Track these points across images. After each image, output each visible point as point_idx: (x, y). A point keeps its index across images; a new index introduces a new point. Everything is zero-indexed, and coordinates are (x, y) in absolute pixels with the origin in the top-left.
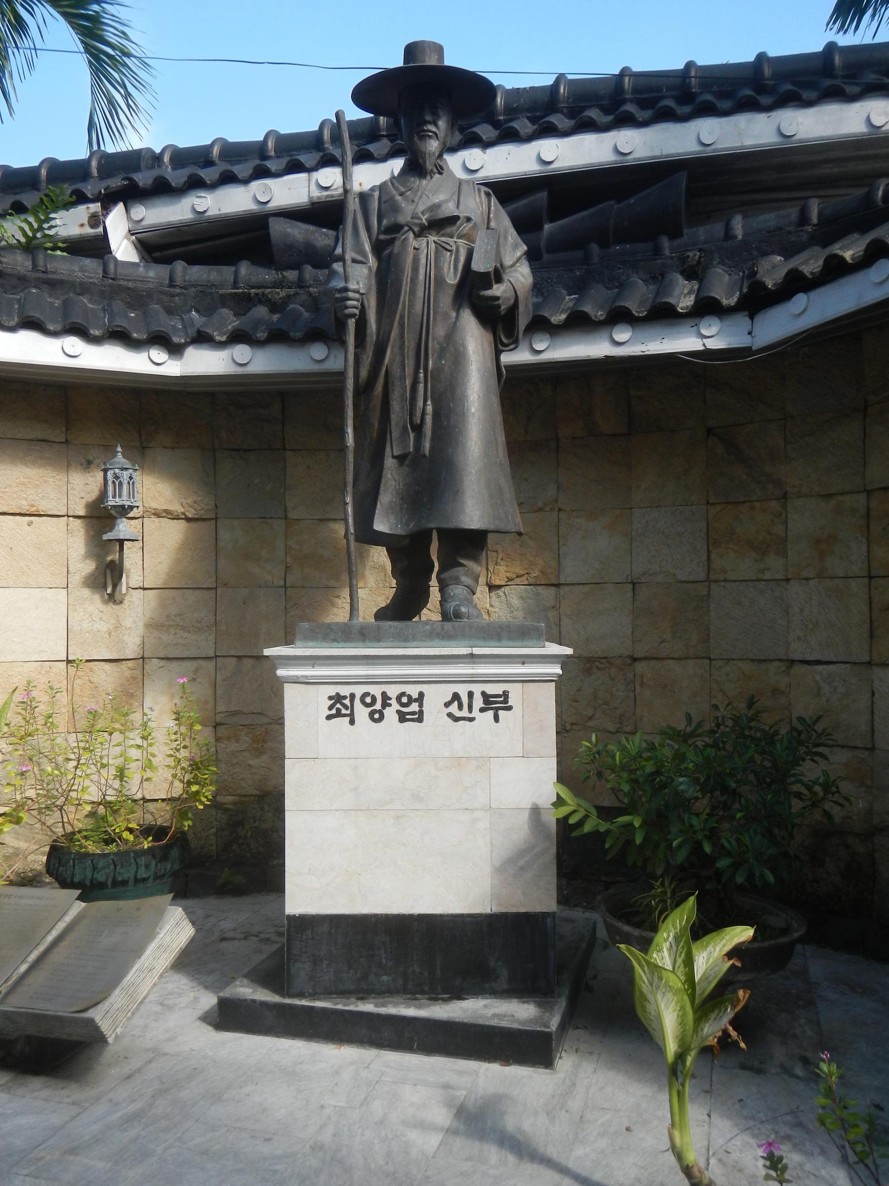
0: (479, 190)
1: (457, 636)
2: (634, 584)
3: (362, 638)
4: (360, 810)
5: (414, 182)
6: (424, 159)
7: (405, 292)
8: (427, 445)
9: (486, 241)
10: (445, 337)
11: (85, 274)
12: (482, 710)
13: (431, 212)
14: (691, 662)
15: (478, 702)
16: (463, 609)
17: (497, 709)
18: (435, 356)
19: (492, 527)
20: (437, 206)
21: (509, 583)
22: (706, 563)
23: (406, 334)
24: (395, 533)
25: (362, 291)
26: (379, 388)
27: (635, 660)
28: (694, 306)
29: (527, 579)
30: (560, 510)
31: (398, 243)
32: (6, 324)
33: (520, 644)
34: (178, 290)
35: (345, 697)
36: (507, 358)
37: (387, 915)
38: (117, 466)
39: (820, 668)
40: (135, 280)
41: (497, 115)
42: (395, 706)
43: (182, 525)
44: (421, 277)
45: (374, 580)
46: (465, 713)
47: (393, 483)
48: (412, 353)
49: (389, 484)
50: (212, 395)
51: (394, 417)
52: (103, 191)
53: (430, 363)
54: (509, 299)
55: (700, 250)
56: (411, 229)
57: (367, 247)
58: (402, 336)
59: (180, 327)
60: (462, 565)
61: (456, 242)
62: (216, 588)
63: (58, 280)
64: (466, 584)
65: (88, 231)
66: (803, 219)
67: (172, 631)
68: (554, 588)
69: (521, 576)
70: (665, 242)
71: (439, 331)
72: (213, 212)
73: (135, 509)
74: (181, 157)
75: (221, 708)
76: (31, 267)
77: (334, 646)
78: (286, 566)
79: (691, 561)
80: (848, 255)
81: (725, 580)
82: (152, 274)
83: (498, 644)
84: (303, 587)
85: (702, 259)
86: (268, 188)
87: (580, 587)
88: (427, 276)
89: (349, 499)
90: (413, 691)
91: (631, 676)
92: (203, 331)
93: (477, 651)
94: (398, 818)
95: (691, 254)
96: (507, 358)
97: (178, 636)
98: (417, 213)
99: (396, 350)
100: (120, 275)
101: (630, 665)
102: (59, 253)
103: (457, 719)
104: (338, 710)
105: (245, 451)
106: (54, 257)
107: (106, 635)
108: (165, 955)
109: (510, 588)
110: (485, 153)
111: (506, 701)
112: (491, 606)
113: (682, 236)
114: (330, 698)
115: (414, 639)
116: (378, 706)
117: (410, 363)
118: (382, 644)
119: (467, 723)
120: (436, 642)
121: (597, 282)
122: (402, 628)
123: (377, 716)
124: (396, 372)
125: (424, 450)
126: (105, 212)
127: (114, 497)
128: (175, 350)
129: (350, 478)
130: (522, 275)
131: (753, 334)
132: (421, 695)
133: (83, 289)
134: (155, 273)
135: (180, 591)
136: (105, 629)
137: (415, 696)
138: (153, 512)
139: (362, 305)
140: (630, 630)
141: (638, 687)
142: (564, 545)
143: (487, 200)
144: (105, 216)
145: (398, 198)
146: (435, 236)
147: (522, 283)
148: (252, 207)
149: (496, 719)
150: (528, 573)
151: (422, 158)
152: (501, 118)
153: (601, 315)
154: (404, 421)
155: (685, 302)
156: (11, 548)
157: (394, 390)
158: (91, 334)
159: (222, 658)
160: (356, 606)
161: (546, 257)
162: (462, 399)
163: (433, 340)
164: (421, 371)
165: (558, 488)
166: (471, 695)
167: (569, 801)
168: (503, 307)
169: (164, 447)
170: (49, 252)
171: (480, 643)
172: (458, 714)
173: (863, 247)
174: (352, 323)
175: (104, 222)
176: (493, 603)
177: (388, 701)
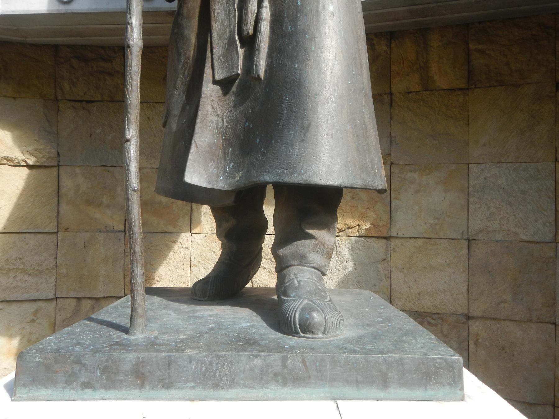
1: (309, 377)
3: (139, 382)
14: (533, 326)
16: (316, 317)
19: (359, 183)
21: (340, 234)
22: (553, 223)
24: (215, 188)
27: (469, 318)
29: (358, 231)
30: (392, 164)
33: (419, 392)
43: (25, 172)
45: (210, 227)
47: (214, 118)
49: (209, 119)
50: (56, 47)
51: (216, 27)
60: (311, 237)
62: (58, 232)
68: (385, 241)
69: (352, 228)
77: (86, 397)
79: (536, 221)
83: (381, 394)
87: (412, 241)
91: (465, 334)
97: (17, 279)
101: (464, 323)
105: (88, 102)
109: (340, 239)
115: (233, 384)
118: (173, 392)
122: (211, 364)
125: (257, 70)
135: (21, 235)
140: (466, 287)
141: (472, 346)
142: (396, 198)
150: (359, 225)
154: (230, 32)
159: (62, 300)
165: (391, 142)
169: (5, 96)
171: (350, 391)
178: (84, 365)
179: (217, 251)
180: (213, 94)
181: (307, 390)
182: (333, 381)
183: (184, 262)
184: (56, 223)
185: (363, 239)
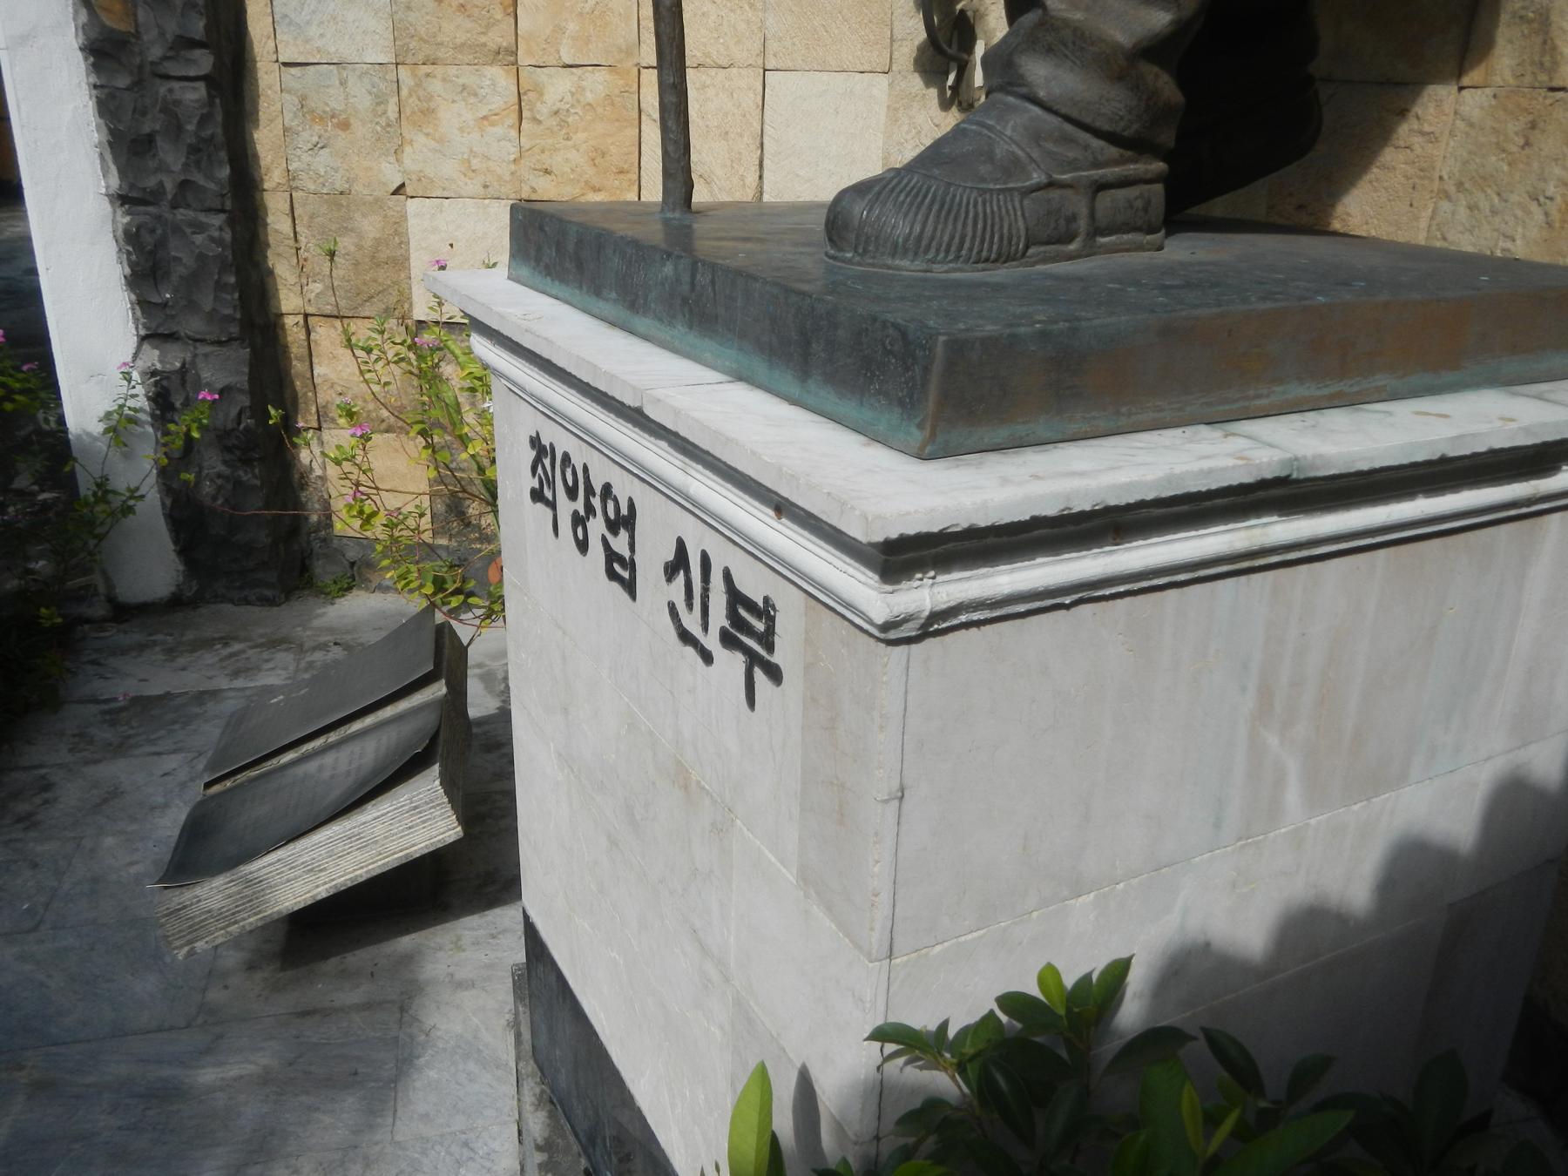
83: (795, 390)
108: (360, 856)
179: (1514, 149)
183: (1417, 181)
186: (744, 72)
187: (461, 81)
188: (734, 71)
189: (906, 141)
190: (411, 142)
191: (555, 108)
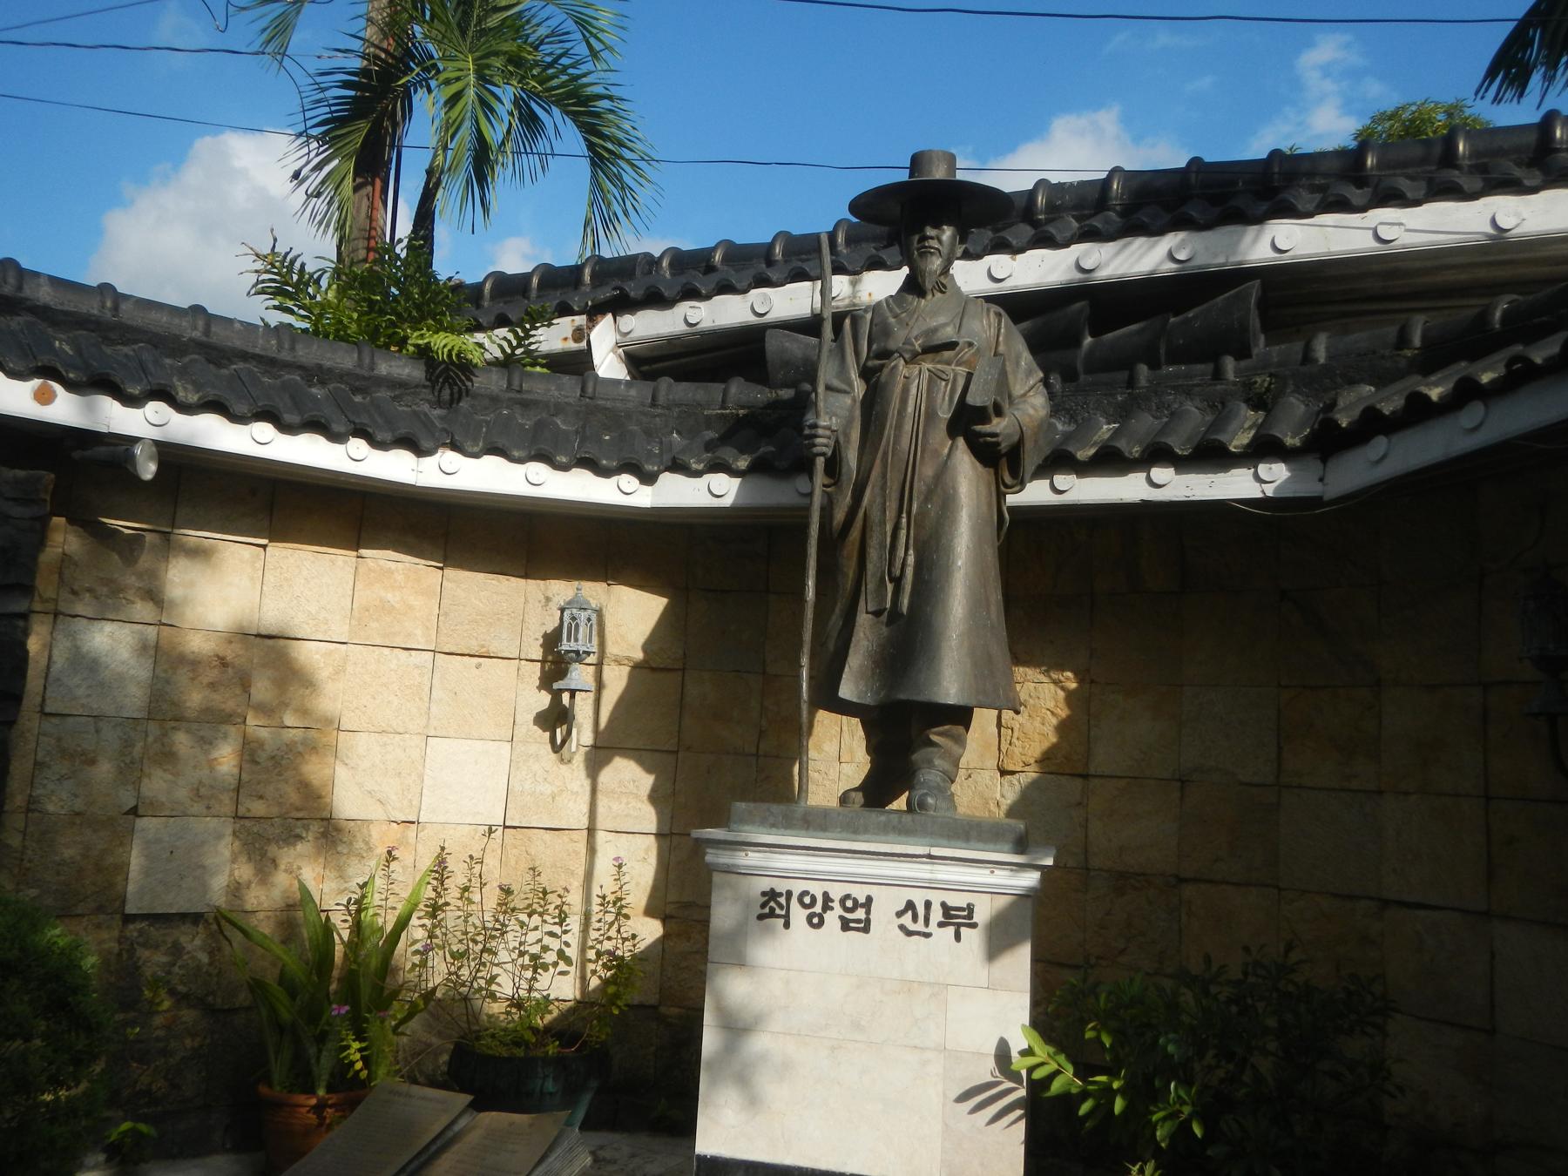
0: (988, 310)
2: (1183, 782)
4: (790, 1034)
5: (911, 303)
6: (923, 277)
7: (891, 427)
8: (905, 602)
9: (987, 369)
10: (934, 478)
11: (562, 393)
12: (941, 925)
13: (926, 337)
15: (937, 915)
16: (930, 800)
17: (959, 926)
18: (922, 497)
20: (935, 330)
21: (1026, 769)
23: (889, 474)
24: (863, 702)
25: (834, 428)
26: (855, 533)
27: (1182, 880)
28: (1249, 445)
31: (886, 371)
32: (470, 450)
33: (991, 846)
34: (659, 411)
35: (780, 895)
36: (1012, 499)
37: (813, 1170)
38: (575, 606)
39: (1422, 913)
40: (614, 400)
41: (1037, 214)
42: (838, 910)
44: (910, 409)
46: (920, 927)
47: (866, 643)
48: (895, 496)
51: (870, 567)
52: (590, 303)
53: (915, 507)
54: (1009, 436)
55: (1271, 375)
56: (901, 356)
57: (854, 375)
58: (884, 476)
59: (657, 452)
61: (953, 370)
62: (677, 752)
63: (532, 400)
64: (941, 769)
65: (572, 345)
66: (1403, 340)
67: (624, 800)
68: (1081, 780)
70: (1229, 364)
71: (927, 471)
72: (707, 324)
73: (592, 655)
74: (683, 261)
75: (672, 897)
76: (505, 386)
78: (761, 732)
80: (1435, 394)
81: (1300, 787)
82: (633, 392)
83: (964, 845)
84: (777, 757)
85: (1273, 386)
86: (767, 298)
88: (917, 408)
89: (805, 661)
90: (860, 893)
92: (678, 459)
93: (936, 851)
94: (833, 1049)
95: (1259, 380)
96: (1012, 499)
97: (630, 806)
98: (910, 339)
99: (877, 490)
100: (599, 393)
102: (538, 369)
103: (909, 933)
104: (772, 910)
106: (531, 374)
107: (550, 799)
110: (1014, 260)
111: (970, 916)
112: (1003, 796)
113: (1249, 356)
114: (764, 894)
115: (866, 831)
116: (818, 909)
117: (892, 506)
118: (827, 834)
119: (923, 938)
120: (891, 837)
121: (1143, 410)
123: (815, 920)
124: (875, 515)
125: (901, 609)
126: (590, 325)
127: (569, 640)
128: (648, 479)
129: (807, 636)
130: (1033, 407)
131: (1326, 481)
132: (869, 899)
133: (559, 409)
134: (643, 391)
136: (549, 792)
137: (862, 900)
138: (613, 658)
139: (837, 442)
143: (996, 321)
144: (590, 329)
145: (892, 320)
146: (930, 363)
147: (1030, 416)
148: (753, 319)
149: (958, 937)
151: (921, 276)
152: (1041, 217)
153: (1136, 451)
155: (1239, 440)
156: (456, 693)
157: (871, 537)
158: (558, 461)
160: (804, 787)
161: (1082, 377)
162: (948, 551)
163: (919, 481)
164: (904, 515)
166: (928, 905)
167: (1037, 1050)
168: (1003, 445)
170: (529, 368)
171: (945, 842)
172: (912, 927)
173: (1451, 385)
174: (820, 461)
175: (589, 335)
176: (1005, 793)
177: (830, 904)
178: (772, 813)
180: (865, 622)
181: (916, 839)
182: (932, 834)
184: (676, 739)
185: (1053, 776)
186: (414, 737)
187: (201, 733)
188: (408, 736)
189: (526, 779)
190: (149, 775)
191: (273, 754)
